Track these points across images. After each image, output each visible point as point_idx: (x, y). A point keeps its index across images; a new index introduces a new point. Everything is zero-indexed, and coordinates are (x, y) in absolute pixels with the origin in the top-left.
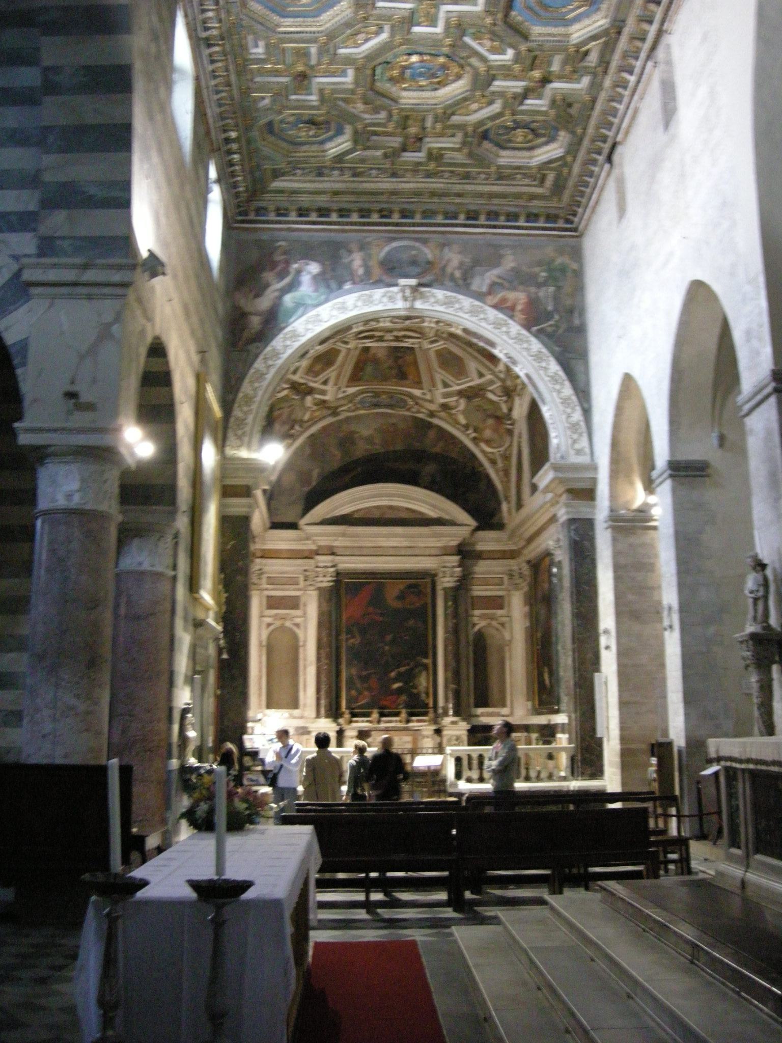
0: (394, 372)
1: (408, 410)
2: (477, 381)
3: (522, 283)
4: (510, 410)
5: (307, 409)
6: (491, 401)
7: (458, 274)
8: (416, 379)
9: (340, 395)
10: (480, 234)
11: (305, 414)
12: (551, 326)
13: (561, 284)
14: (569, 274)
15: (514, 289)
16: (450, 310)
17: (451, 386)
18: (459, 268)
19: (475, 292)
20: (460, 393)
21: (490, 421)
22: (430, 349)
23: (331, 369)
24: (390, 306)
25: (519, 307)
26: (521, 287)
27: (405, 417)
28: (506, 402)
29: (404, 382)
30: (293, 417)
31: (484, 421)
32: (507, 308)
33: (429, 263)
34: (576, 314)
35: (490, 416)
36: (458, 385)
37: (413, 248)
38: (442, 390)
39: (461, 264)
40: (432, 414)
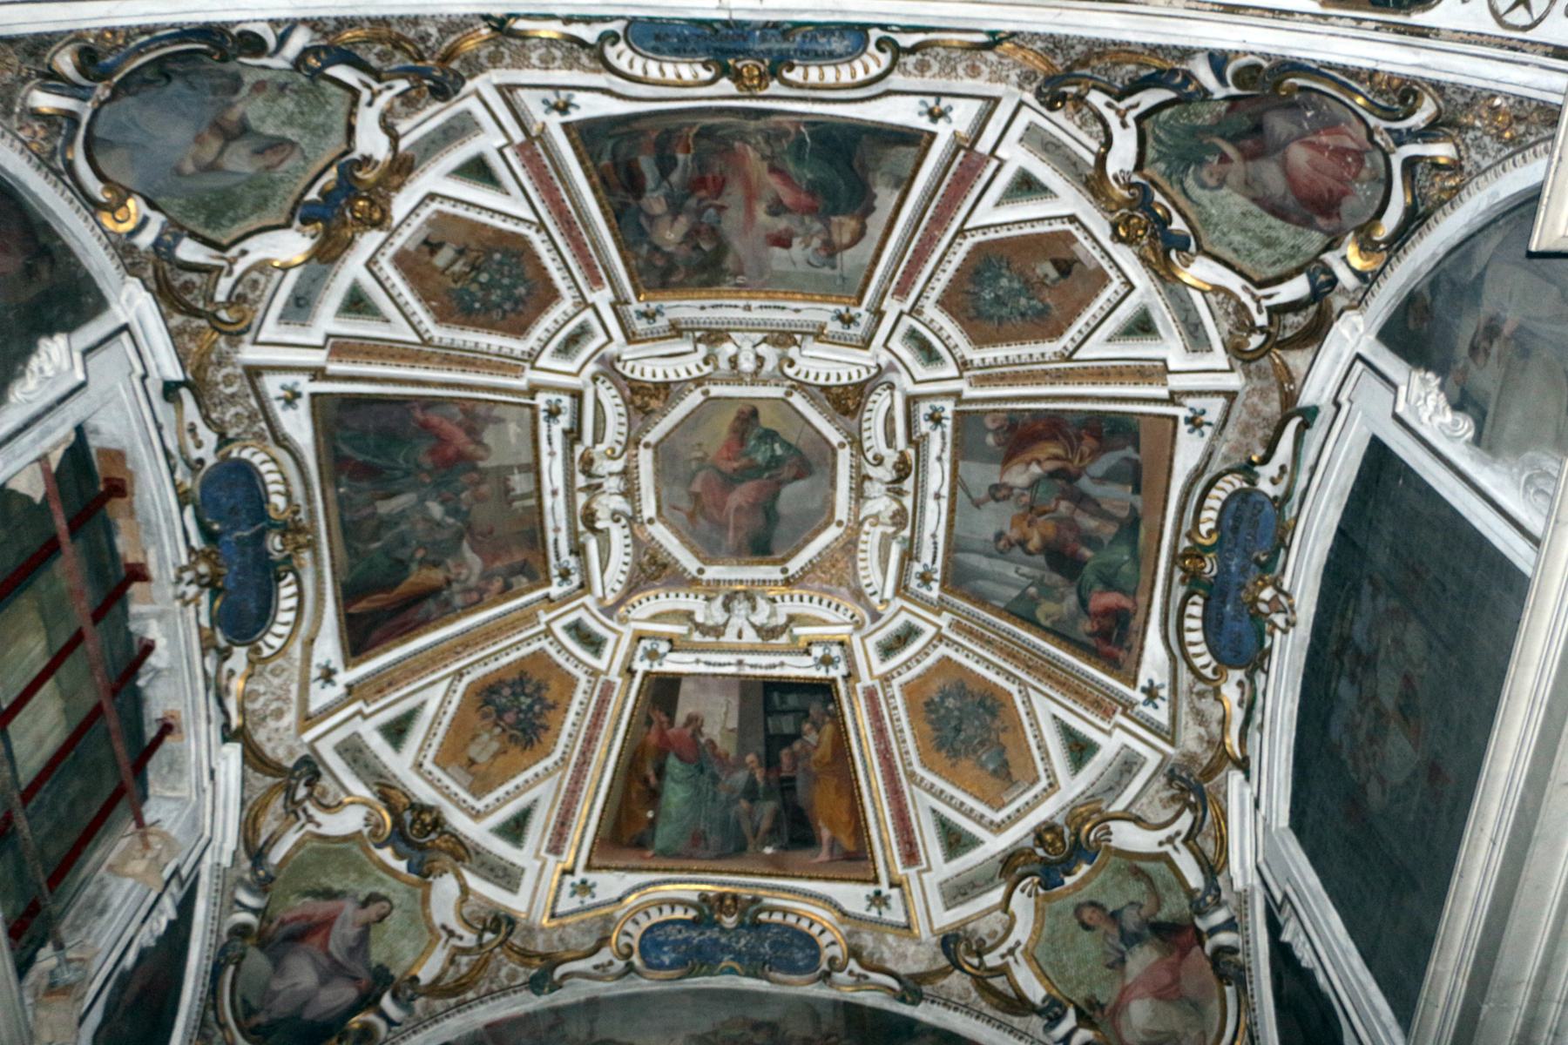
0: (767, 808)
1: (826, 976)
2: (1073, 786)
4: (1213, 868)
5: (433, 933)
6: (1134, 865)
8: (847, 843)
9: (567, 903)
11: (425, 954)
17: (974, 842)
20: (1011, 866)
21: (1142, 959)
22: (886, 679)
23: (539, 768)
27: (811, 1007)
28: (1190, 838)
29: (800, 856)
30: (377, 954)
31: (1119, 964)
35: (1131, 939)
36: (998, 828)
38: (940, 868)
40: (913, 987)
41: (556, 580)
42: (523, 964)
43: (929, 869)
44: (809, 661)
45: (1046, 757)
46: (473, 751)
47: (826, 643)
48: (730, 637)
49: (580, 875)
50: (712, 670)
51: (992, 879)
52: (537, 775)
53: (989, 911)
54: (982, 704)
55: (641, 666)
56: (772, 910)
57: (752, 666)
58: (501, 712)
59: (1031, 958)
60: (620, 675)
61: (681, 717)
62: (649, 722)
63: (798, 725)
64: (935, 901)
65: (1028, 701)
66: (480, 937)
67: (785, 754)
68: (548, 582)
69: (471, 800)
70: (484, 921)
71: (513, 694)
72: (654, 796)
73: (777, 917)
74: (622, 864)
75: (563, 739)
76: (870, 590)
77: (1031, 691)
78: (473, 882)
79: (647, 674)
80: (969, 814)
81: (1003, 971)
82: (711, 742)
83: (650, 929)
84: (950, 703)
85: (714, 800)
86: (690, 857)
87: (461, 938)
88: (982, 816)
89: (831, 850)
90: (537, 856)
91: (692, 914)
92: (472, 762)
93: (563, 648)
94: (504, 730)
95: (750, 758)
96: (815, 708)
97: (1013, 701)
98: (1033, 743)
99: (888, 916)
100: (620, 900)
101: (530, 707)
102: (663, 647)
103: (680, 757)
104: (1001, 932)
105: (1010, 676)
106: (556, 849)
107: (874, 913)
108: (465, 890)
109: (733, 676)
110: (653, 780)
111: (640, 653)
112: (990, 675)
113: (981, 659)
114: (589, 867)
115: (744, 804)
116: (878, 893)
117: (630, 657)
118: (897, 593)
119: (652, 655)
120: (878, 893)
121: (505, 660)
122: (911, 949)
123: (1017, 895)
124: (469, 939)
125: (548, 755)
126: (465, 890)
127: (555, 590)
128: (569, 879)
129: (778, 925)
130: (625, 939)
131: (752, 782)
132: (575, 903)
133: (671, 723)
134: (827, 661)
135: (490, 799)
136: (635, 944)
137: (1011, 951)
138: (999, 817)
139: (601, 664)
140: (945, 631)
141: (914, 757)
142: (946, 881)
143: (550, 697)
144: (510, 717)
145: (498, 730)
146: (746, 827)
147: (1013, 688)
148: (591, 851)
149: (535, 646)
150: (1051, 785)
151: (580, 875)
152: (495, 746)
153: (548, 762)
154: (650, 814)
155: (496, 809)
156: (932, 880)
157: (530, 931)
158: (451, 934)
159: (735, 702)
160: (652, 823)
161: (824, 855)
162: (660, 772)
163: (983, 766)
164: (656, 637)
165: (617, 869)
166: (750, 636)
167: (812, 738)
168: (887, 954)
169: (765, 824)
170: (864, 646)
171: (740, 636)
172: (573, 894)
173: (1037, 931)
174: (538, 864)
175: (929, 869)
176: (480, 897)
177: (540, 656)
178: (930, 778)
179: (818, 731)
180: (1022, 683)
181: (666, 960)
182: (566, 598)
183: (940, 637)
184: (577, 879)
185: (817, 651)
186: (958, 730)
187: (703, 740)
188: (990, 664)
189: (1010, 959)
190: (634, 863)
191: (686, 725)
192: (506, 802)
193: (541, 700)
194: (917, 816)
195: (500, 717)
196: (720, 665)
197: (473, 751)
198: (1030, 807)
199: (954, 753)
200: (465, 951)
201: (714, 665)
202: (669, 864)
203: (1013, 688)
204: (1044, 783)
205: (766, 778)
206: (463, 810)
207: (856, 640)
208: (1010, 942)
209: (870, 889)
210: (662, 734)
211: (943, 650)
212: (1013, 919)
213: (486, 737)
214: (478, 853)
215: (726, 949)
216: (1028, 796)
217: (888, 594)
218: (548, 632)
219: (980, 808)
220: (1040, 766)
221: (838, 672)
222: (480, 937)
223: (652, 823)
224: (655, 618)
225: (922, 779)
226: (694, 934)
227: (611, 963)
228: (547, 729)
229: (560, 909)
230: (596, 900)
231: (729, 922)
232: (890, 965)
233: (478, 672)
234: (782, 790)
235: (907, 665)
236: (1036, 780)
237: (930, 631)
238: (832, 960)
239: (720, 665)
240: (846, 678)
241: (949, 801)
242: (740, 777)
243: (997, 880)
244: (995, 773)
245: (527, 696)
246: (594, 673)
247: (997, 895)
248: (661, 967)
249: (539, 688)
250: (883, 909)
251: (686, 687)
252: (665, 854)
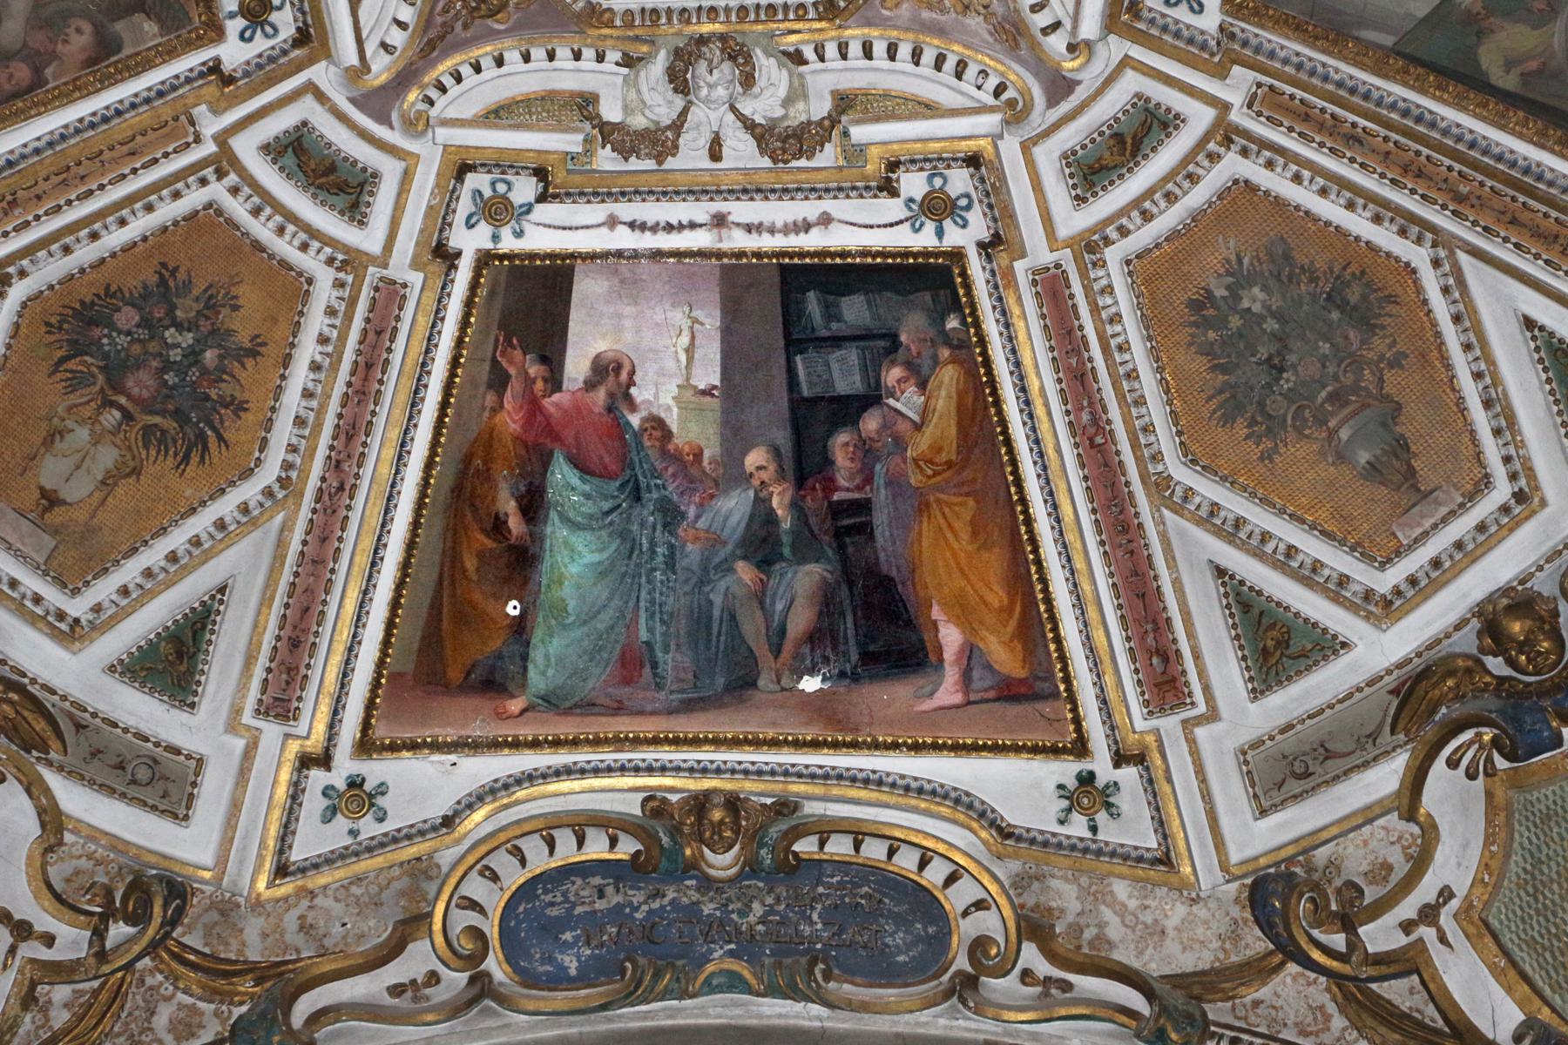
1: (965, 988)
9: (313, 839)
17: (1328, 646)
22: (1090, 246)
41: (234, 26)
42: (212, 995)
43: (1212, 716)
44: (892, 208)
45: (1507, 425)
46: (51, 472)
47: (934, 163)
48: (690, 156)
49: (345, 765)
51: (1373, 737)
52: (221, 525)
53: (1369, 815)
54: (1335, 299)
55: (470, 241)
56: (825, 830)
57: (749, 228)
58: (116, 371)
59: (1481, 929)
60: (416, 265)
61: (576, 367)
62: (499, 381)
63: (872, 371)
64: (1231, 793)
65: (1456, 287)
66: (99, 934)
67: (841, 445)
68: (216, 32)
69: (53, 596)
70: (109, 893)
71: (145, 323)
73: (839, 847)
74: (450, 734)
75: (283, 432)
76: (1042, 20)
77: (1463, 257)
78: (73, 798)
79: (485, 259)
80: (1310, 576)
81: (1410, 962)
82: (657, 424)
83: (526, 891)
84: (1254, 299)
85: (670, 563)
86: (619, 709)
87: (49, 940)
88: (1344, 580)
89: (966, 679)
90: (233, 726)
91: (628, 847)
92: (51, 500)
93: (265, 202)
94: (128, 416)
95: (755, 458)
96: (912, 328)
97: (1419, 289)
98: (1471, 391)
99: (1110, 833)
100: (448, 822)
101: (193, 355)
102: (524, 189)
103: (580, 464)
104: (1401, 868)
105: (1408, 225)
106: (280, 707)
107: (1078, 827)
108: (52, 820)
109: (701, 254)
110: (515, 524)
111: (464, 206)
112: (1359, 225)
113: (1332, 185)
114: (366, 746)
115: (745, 572)
116: (1087, 779)
117: (441, 217)
118: (1111, 24)
119: (496, 210)
120: (1087, 779)
121: (116, 238)
122: (1176, 913)
123: (1440, 780)
124: (71, 940)
125: (247, 473)
126: (52, 820)
127: (233, 52)
128: (317, 778)
129: (842, 865)
130: (472, 918)
131: (763, 516)
132: (336, 835)
133: (555, 381)
134: (937, 207)
135: (104, 590)
136: (492, 931)
137: (1429, 914)
138: (1385, 581)
139: (369, 239)
140: (1237, 117)
141: (1165, 439)
142: (1257, 744)
143: (242, 328)
144: (141, 383)
145: (112, 417)
146: (753, 628)
147: (1418, 256)
148: (370, 706)
149: (194, 198)
150: (1520, 497)
151: (345, 765)
152: (107, 457)
153: (249, 491)
154: (513, 609)
155: (122, 614)
156: (1219, 743)
157: (226, 909)
158: (23, 930)
159: (711, 320)
160: (520, 627)
161: (948, 692)
162: (533, 504)
163: (1341, 457)
164: (503, 164)
165: (437, 747)
166: (742, 152)
167: (908, 402)
168: (1115, 930)
169: (800, 621)
170: (1031, 164)
171: (715, 155)
172: (329, 814)
173: (1492, 868)
174: (239, 744)
175: (1212, 716)
176: (95, 834)
177: (209, 220)
178: (1208, 489)
179: (922, 385)
180: (1440, 239)
181: (572, 965)
182: (266, 71)
183: (1225, 133)
184: (337, 778)
185: (914, 184)
186: (1276, 367)
187: (635, 420)
188: (1355, 197)
189: (1427, 933)
190: (478, 730)
191: (590, 385)
192: (147, 595)
193: (218, 335)
194: (1177, 584)
195: (117, 386)
196: (669, 228)
197: (51, 472)
198: (1466, 553)
199: (1268, 426)
200: (61, 971)
201: (654, 229)
202: (566, 727)
203: (1418, 256)
204: (1502, 491)
205: (796, 506)
206: (33, 620)
207: (1010, 149)
208: (1425, 891)
209: (1066, 770)
210: (533, 407)
211: (1233, 165)
212: (1430, 833)
213: (82, 434)
214: (80, 727)
215: (718, 929)
216: (1461, 527)
217: (1090, 27)
218: (224, 162)
219: (1337, 560)
220: (1492, 451)
221: (965, 235)
222: (99, 934)
223: (520, 627)
224: (496, 115)
225: (1189, 492)
226: (637, 897)
227: (433, 978)
228: (240, 408)
229: (296, 855)
230: (389, 826)
231: (722, 863)
232: (1123, 955)
233: (50, 270)
234: (839, 534)
235: (1142, 208)
236: (1485, 483)
237: (1200, 117)
238: (979, 945)
239: (669, 228)
240: (987, 248)
241: (1259, 544)
242: (734, 507)
243: (1386, 737)
244: (1374, 471)
245: (179, 326)
246: (350, 262)
247: (1386, 777)
248: (558, 981)
249: (211, 305)
250: (1102, 817)
251: (587, 288)
252: (552, 703)
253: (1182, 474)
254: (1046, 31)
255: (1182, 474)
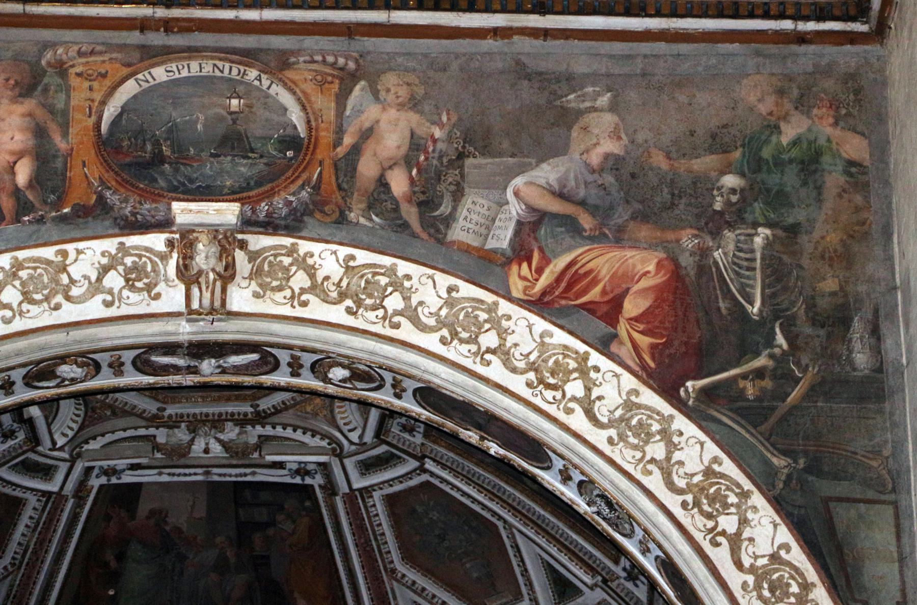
3: (642, 217)
7: (399, 183)
10: (496, 32)
12: (759, 373)
13: (798, 215)
14: (834, 179)
15: (619, 238)
16: (368, 320)
18: (408, 161)
19: (467, 249)
22: (367, 491)
24: (136, 303)
25: (632, 307)
26: (644, 232)
32: (590, 308)
33: (291, 142)
34: (858, 327)
37: (234, 87)
39: (416, 144)
50: (176, 479)
67: (257, 538)
72: (114, 577)
82: (179, 530)
110: (113, 564)
115: (214, 577)
133: (133, 517)
141: (395, 556)
154: (111, 593)
162: (121, 557)
178: (412, 575)
180: (505, 521)
186: (442, 538)
217: (369, 437)
220: (524, 590)
242: (210, 556)
253: (401, 568)
254: (350, 431)
255: (401, 568)
